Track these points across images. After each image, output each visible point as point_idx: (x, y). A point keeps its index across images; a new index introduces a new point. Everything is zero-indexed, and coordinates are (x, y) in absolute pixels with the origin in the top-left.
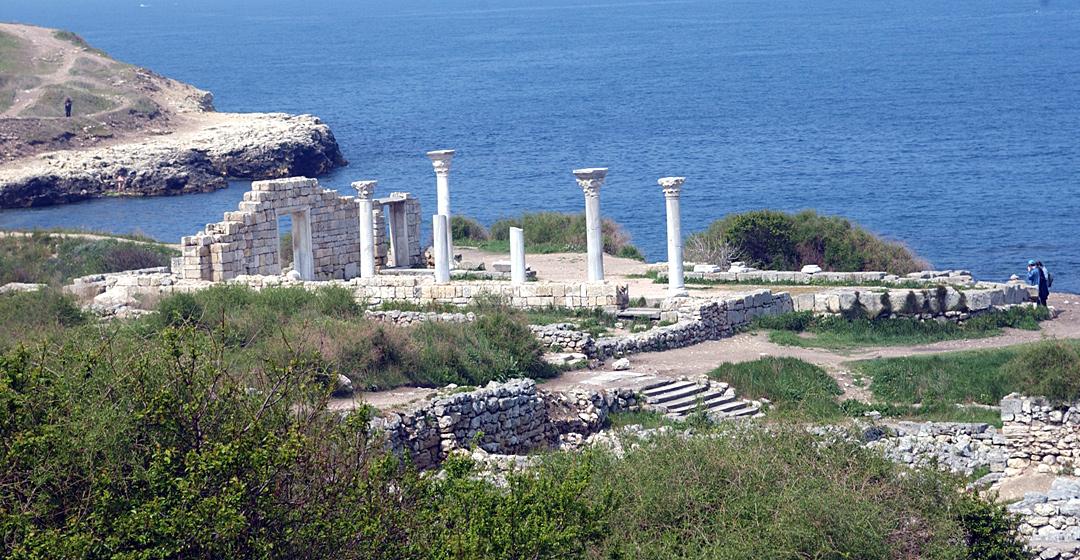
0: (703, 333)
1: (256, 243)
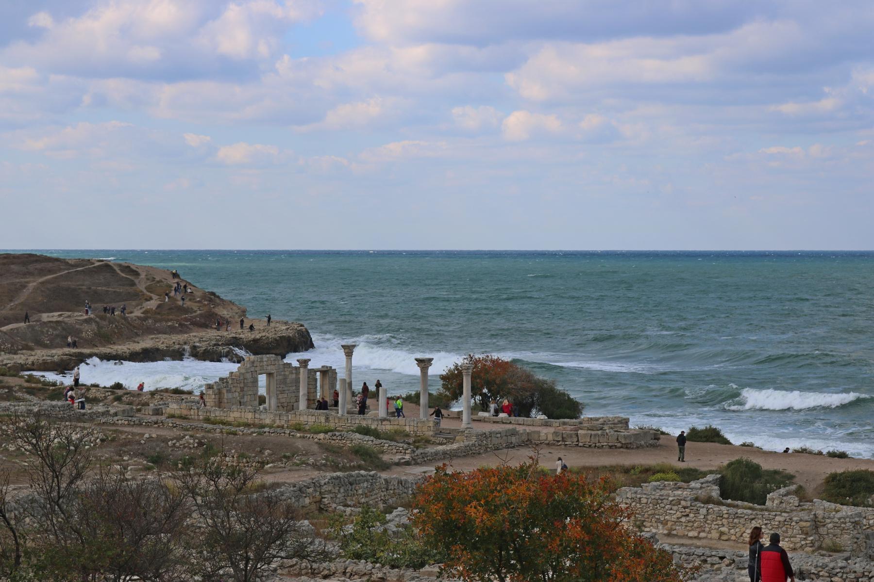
1: (246, 389)
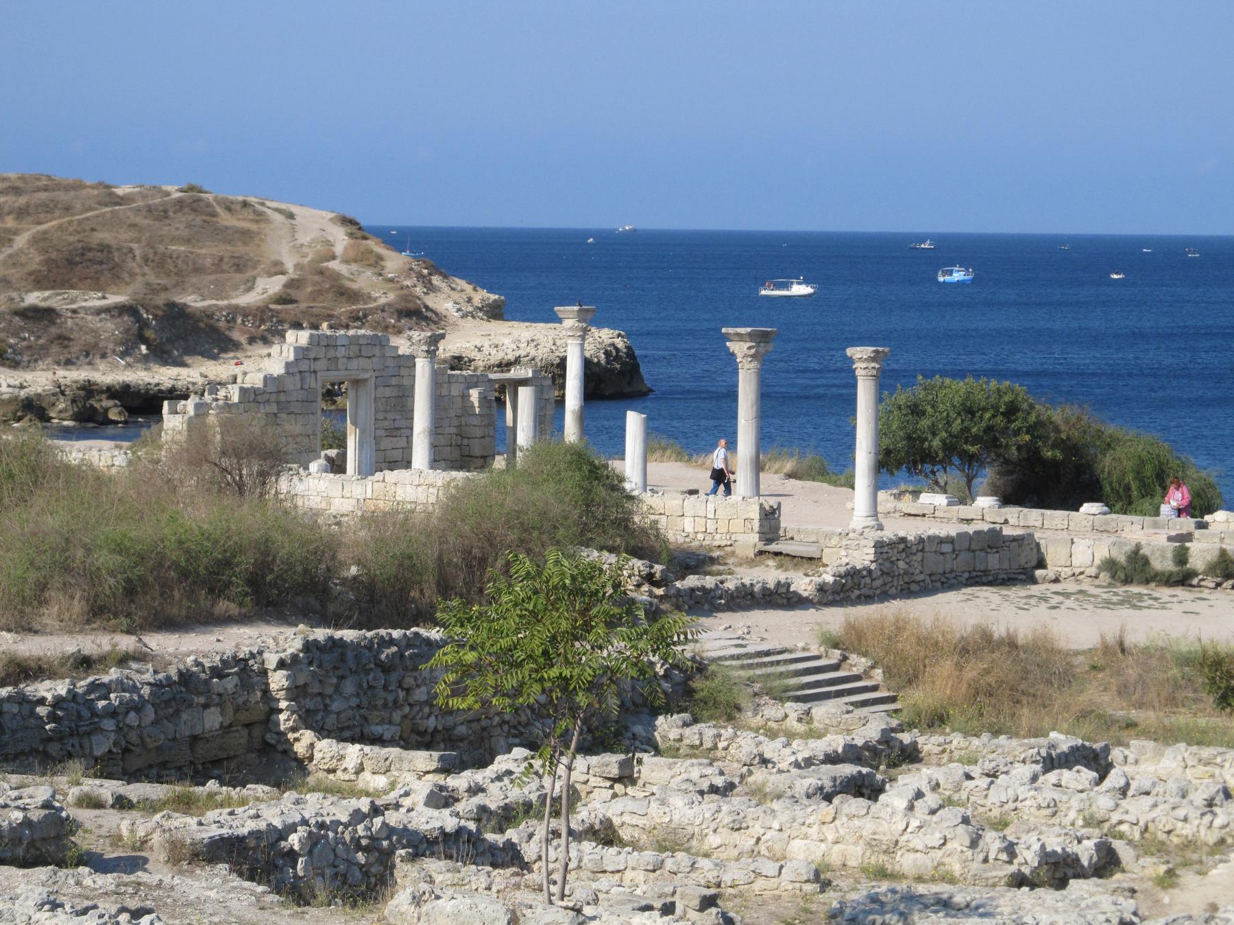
0: (878, 583)
